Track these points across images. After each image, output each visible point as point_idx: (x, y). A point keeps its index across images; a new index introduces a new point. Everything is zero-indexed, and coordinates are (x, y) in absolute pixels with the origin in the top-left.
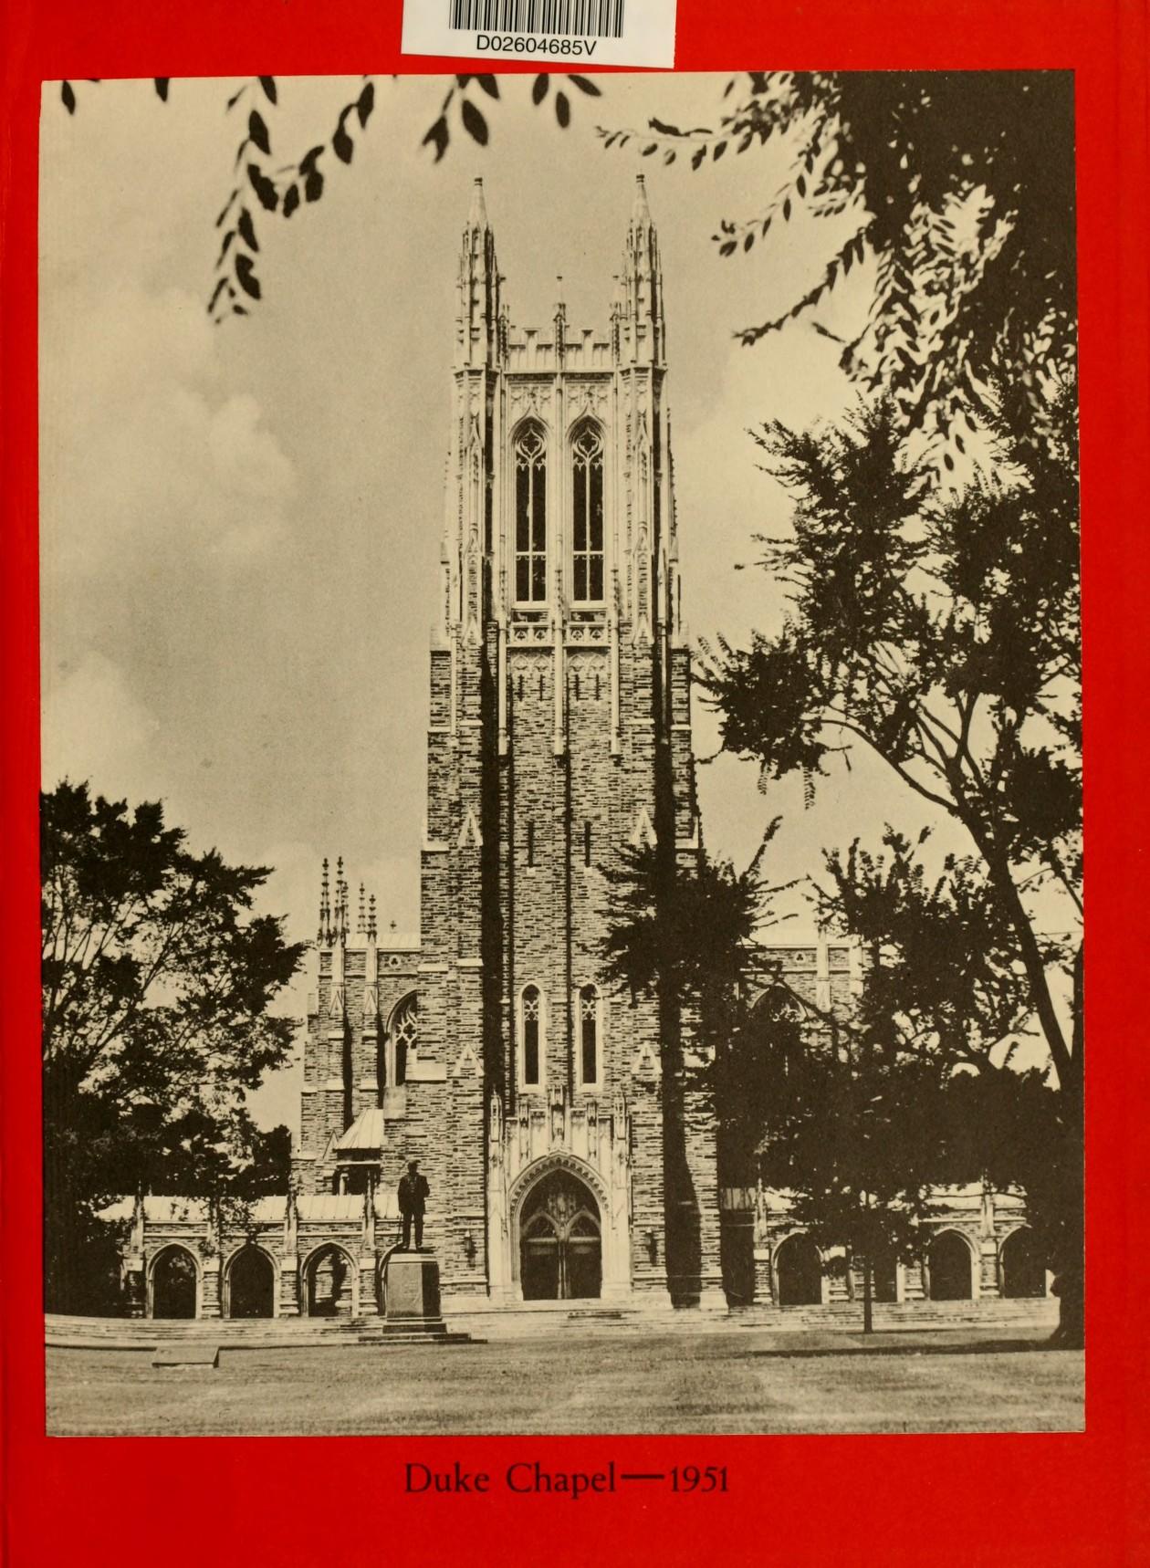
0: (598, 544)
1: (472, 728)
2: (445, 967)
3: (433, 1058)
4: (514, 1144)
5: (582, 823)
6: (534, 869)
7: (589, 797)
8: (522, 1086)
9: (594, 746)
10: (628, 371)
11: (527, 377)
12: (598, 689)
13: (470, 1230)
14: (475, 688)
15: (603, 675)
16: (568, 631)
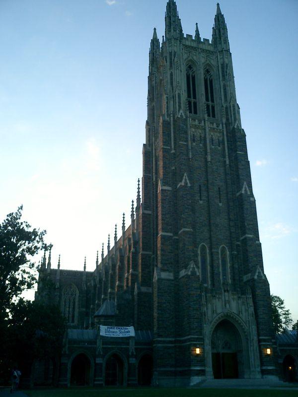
0: (213, 101)
2: (171, 234)
3: (168, 270)
10: (222, 51)
11: (189, 47)
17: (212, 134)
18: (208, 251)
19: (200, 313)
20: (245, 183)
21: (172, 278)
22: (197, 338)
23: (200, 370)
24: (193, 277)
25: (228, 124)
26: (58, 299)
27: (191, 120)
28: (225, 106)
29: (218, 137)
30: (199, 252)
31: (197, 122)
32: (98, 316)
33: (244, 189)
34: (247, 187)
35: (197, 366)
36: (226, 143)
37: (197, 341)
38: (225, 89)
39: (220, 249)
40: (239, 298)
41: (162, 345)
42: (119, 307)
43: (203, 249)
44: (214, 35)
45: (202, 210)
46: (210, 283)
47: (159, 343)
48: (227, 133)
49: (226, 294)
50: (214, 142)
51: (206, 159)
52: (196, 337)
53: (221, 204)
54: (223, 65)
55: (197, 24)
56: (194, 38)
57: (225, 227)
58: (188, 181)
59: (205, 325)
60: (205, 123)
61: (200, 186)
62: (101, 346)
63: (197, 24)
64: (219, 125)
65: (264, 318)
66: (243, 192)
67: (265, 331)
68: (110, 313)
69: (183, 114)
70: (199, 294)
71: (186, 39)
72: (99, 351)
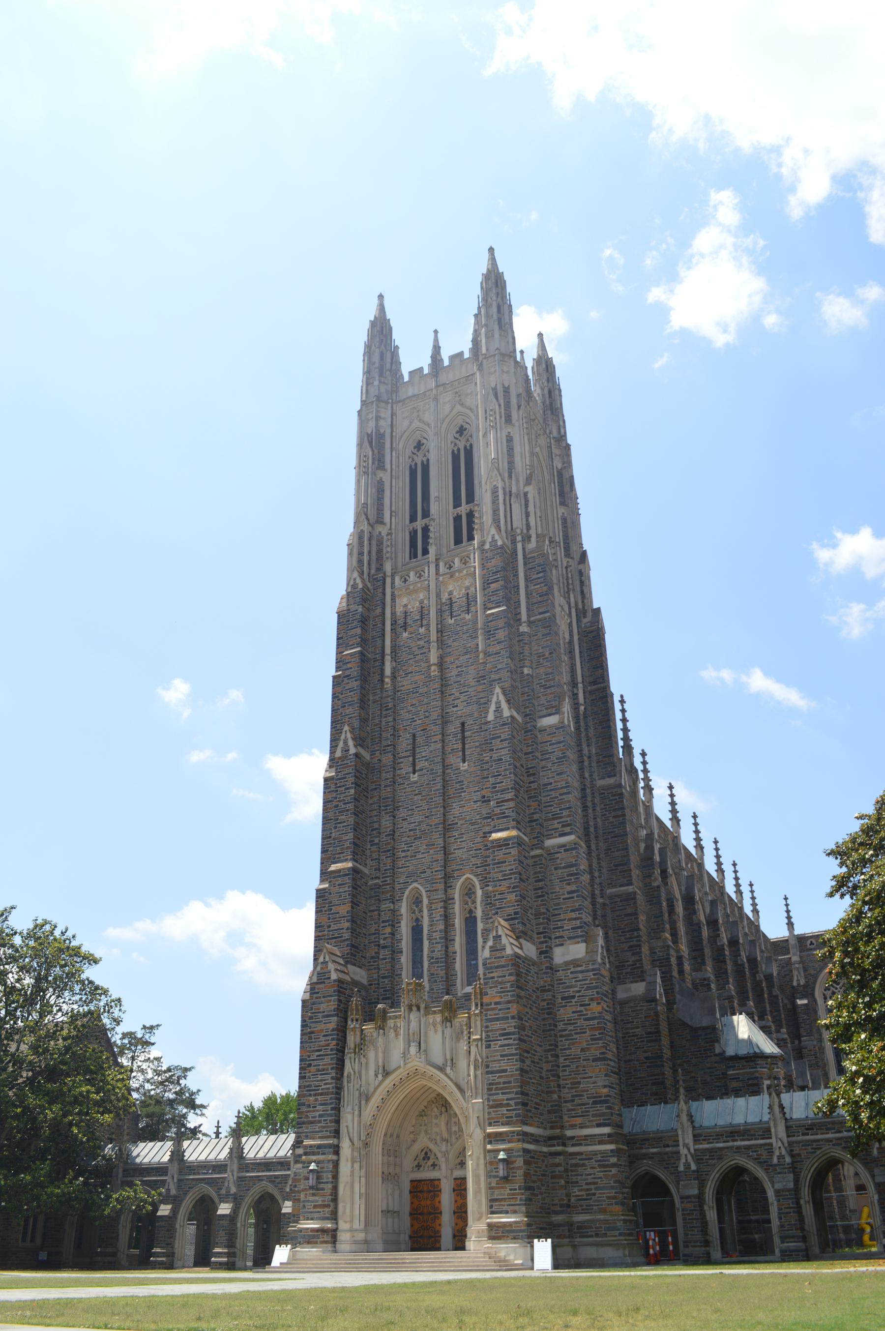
0: (470, 499)
1: (351, 655)
4: (371, 1055)
5: (458, 723)
7: (463, 699)
9: (466, 653)
12: (468, 605)
14: (356, 623)
16: (441, 564)
19: (332, 1078)
20: (498, 690)
22: (319, 1147)
23: (317, 1230)
24: (322, 986)
29: (467, 588)
30: (404, 910)
33: (493, 707)
34: (502, 698)
37: (318, 1154)
45: (416, 797)
49: (414, 1016)
50: (455, 607)
51: (428, 661)
52: (319, 1142)
53: (464, 767)
55: (436, 332)
57: (472, 824)
58: (351, 743)
61: (414, 736)
65: (506, 1071)
66: (491, 717)
67: (504, 1110)
69: (358, 581)
70: (333, 1030)
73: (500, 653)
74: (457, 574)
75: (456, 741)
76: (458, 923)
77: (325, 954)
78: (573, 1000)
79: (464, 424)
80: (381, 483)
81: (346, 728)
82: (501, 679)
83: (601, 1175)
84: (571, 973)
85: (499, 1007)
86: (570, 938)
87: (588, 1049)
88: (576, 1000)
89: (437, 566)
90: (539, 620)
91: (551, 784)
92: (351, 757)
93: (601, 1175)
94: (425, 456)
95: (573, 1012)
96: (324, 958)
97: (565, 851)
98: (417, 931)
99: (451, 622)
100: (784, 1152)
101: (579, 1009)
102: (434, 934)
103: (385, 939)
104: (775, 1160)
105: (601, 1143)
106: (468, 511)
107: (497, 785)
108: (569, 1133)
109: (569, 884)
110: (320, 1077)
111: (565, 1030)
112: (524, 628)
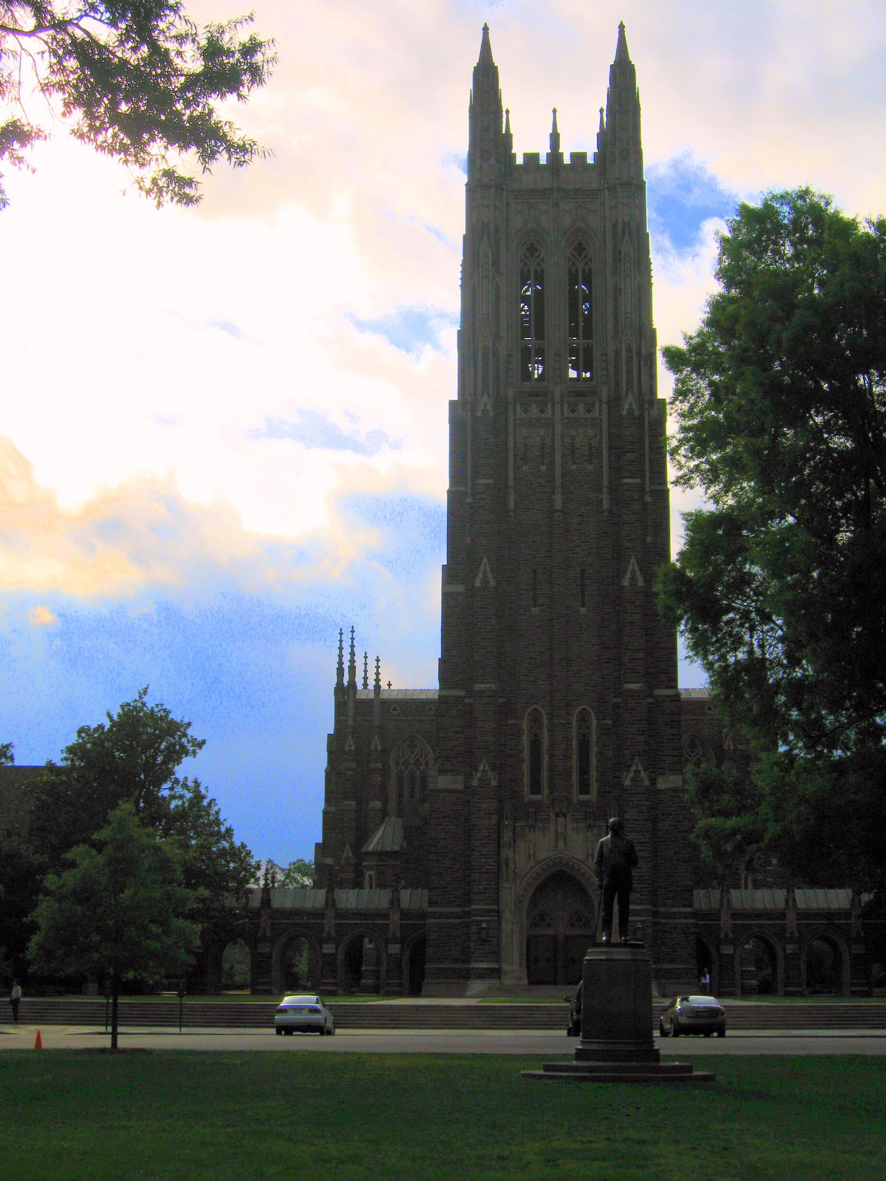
0: (588, 334)
2: (462, 693)
3: (452, 771)
6: (537, 609)
8: (528, 796)
13: (487, 922)
15: (594, 442)
16: (566, 406)
17: (573, 432)
18: (546, 722)
19: (495, 862)
20: (633, 560)
21: (460, 787)
22: (486, 911)
23: (487, 969)
25: (615, 402)
26: (379, 779)
27: (518, 406)
28: (611, 349)
30: (525, 726)
31: (534, 411)
32: (368, 854)
33: (628, 575)
34: (636, 567)
35: (482, 961)
36: (605, 454)
37: (485, 916)
38: (616, 300)
39: (575, 715)
40: (589, 826)
41: (434, 920)
42: (408, 833)
43: (535, 719)
44: (603, 138)
46: (546, 791)
47: (431, 918)
48: (609, 427)
49: (561, 820)
53: (583, 611)
54: (615, 226)
55: (554, 111)
56: (543, 161)
59: (507, 885)
60: (553, 411)
61: (535, 571)
62: (334, 922)
63: (554, 111)
64: (593, 405)
66: (626, 583)
68: (388, 848)
69: (489, 407)
70: (494, 825)
71: (524, 167)
72: (329, 930)
73: (633, 524)
74: (582, 421)
75: (576, 585)
76: (575, 743)
77: (484, 764)
78: (670, 817)
79: (583, 242)
80: (498, 287)
81: (485, 560)
82: (634, 549)
83: (683, 939)
84: (671, 797)
85: (637, 823)
86: (670, 770)
87: (680, 853)
88: (673, 816)
89: (562, 406)
90: (659, 491)
91: (661, 643)
92: (492, 589)
93: (683, 939)
94: (539, 265)
95: (670, 825)
96: (484, 767)
97: (670, 701)
98: (535, 745)
99: (574, 467)
100: (795, 930)
101: (674, 823)
102: (558, 752)
103: (511, 749)
104: (788, 935)
105: (685, 918)
106: (586, 345)
107: (631, 644)
108: (662, 910)
109: (671, 728)
110: (483, 860)
111: (663, 838)
112: (648, 499)
